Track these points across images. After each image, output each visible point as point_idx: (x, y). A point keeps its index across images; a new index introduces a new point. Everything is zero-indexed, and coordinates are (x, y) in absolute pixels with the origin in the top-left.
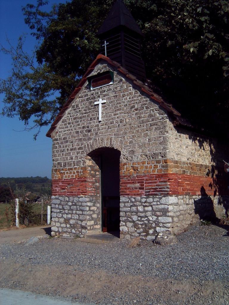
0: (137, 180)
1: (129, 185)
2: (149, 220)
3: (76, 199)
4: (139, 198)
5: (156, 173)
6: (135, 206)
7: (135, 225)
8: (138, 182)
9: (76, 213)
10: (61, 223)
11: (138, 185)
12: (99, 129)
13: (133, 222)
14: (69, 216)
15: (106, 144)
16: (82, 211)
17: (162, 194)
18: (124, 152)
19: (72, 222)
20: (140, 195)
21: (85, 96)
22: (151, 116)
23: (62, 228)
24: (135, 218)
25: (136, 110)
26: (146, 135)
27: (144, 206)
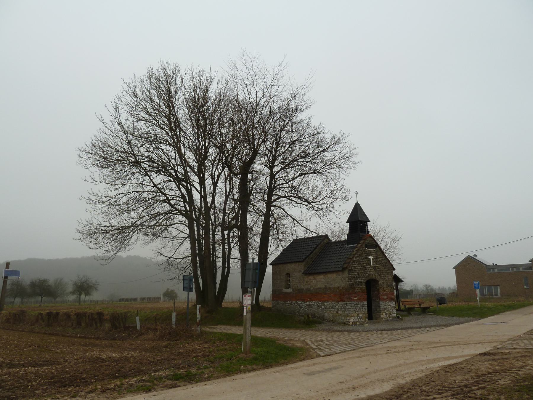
1: (383, 297)
2: (390, 311)
3: (362, 303)
4: (386, 302)
6: (385, 305)
7: (386, 314)
9: (362, 311)
10: (355, 317)
11: (386, 297)
12: (370, 270)
13: (385, 312)
14: (359, 312)
15: (374, 277)
16: (365, 309)
18: (381, 282)
19: (361, 315)
20: (386, 301)
21: (363, 251)
22: (388, 269)
23: (356, 319)
24: (386, 311)
25: (384, 265)
26: (387, 277)
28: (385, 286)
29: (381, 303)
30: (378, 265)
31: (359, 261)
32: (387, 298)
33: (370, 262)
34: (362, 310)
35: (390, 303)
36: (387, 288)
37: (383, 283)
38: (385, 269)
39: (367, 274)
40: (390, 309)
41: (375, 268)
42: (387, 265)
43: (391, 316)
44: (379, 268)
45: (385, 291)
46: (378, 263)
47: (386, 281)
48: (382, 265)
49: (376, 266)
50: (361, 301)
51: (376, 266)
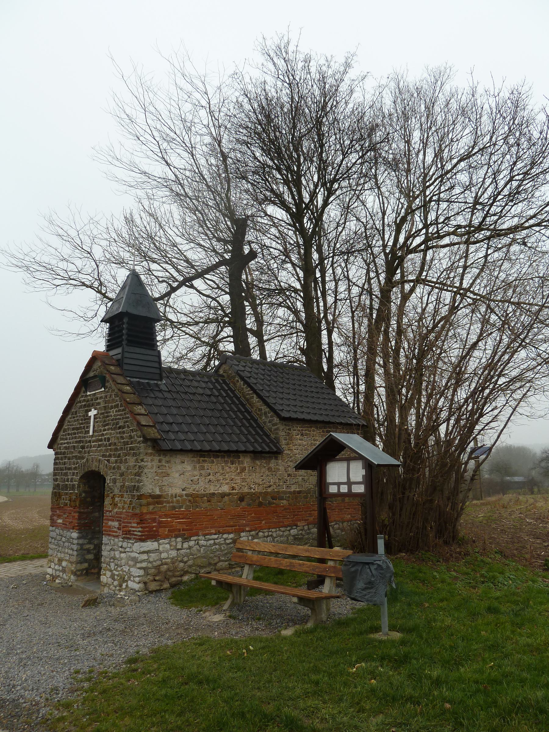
0: (117, 517)
4: (116, 540)
5: (131, 511)
7: (112, 577)
8: (118, 521)
17: (134, 538)
20: (117, 537)
22: (131, 437)
27: (121, 552)
28: (116, 491)
29: (105, 539)
30: (108, 429)
31: (73, 429)
32: (119, 529)
33: (88, 427)
34: (66, 551)
35: (125, 545)
36: (122, 496)
37: (114, 481)
38: (122, 438)
39: (83, 458)
40: (123, 562)
41: (101, 440)
42: (128, 427)
43: (124, 586)
44: (109, 439)
45: (115, 505)
46: (107, 425)
47: (122, 475)
48: (115, 429)
49: (103, 435)
50: (68, 529)
51: (103, 435)
